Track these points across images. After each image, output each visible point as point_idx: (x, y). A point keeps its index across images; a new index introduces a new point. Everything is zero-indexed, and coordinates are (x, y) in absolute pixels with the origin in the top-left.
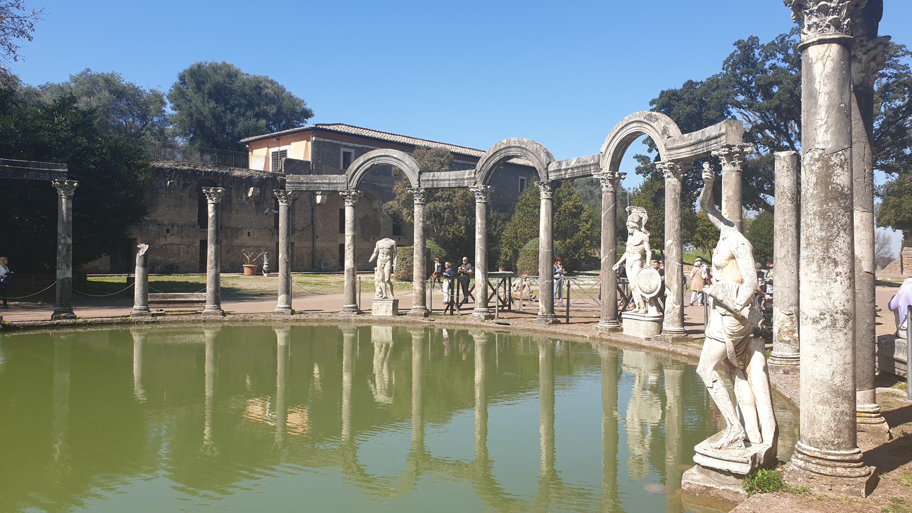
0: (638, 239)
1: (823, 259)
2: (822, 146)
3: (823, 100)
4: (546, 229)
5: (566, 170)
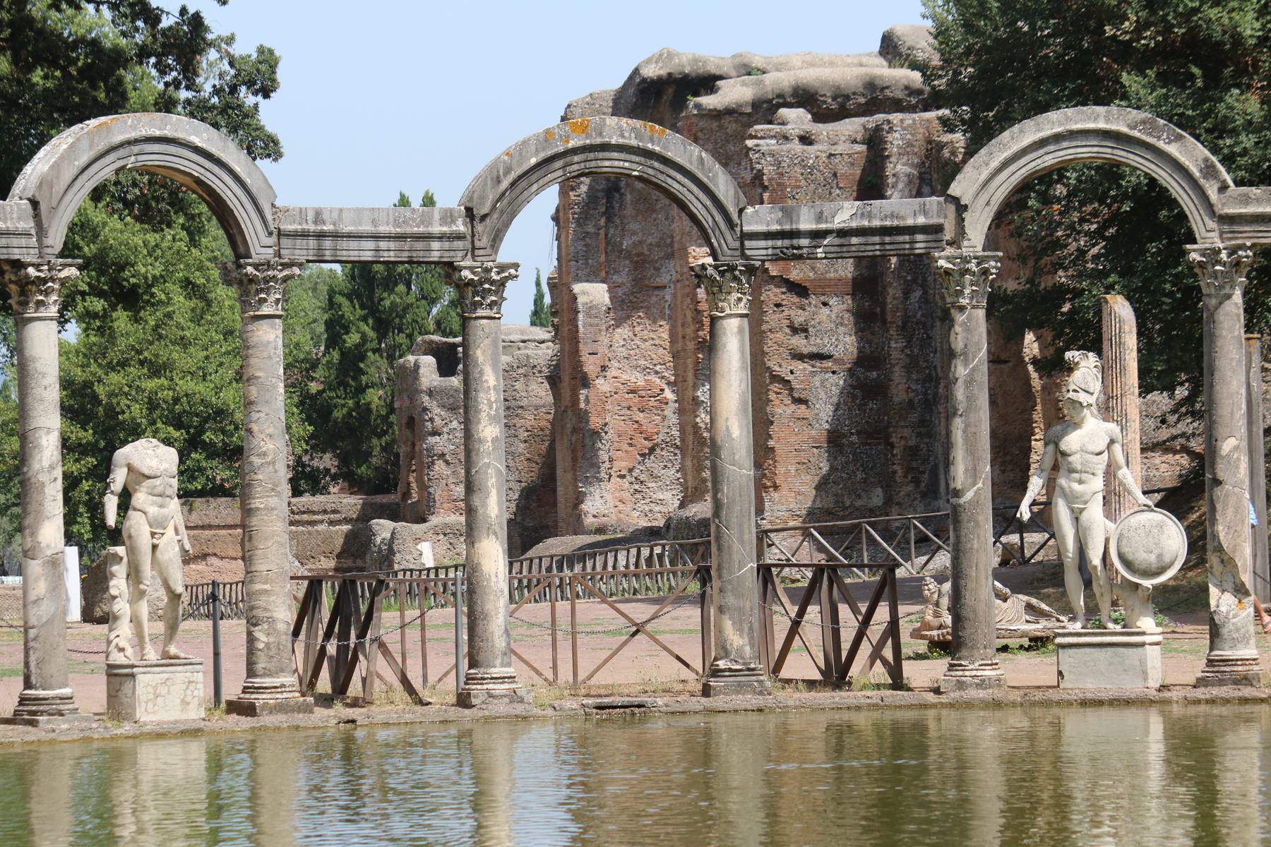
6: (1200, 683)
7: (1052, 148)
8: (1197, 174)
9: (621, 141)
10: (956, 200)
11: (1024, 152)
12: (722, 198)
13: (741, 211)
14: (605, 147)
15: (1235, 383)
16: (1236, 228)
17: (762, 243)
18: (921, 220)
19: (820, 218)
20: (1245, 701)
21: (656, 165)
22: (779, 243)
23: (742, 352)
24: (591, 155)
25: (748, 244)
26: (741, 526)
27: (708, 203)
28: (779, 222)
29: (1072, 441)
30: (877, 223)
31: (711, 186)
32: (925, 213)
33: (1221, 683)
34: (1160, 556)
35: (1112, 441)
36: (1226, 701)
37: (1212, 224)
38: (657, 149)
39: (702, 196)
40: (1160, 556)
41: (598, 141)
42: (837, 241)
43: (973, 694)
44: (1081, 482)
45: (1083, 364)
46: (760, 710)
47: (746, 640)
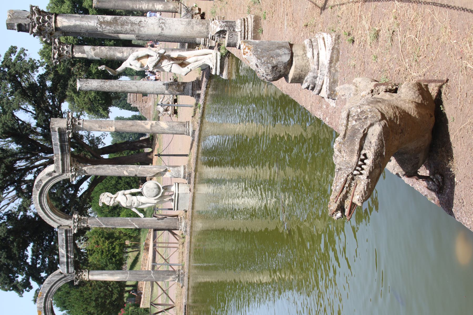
0: (122, 198)
1: (139, 25)
2: (96, 24)
3: (78, 23)
4: (112, 274)
5: (68, 257)
6: (189, 183)
7: (44, 207)
8: (51, 178)
9: (43, 303)
10: (58, 227)
11: (45, 213)
12: (58, 279)
13: (61, 273)
14: (45, 307)
15: (109, 171)
16: (66, 169)
17: (70, 269)
18: (64, 234)
19: (63, 256)
20: (195, 177)
21: (49, 294)
22: (70, 265)
23: (98, 275)
24: (47, 310)
25: (70, 272)
26: (142, 277)
27: (59, 282)
28: (64, 265)
29: (124, 204)
30: (65, 244)
31: (55, 281)
32: (62, 233)
33: (190, 179)
34: (155, 188)
35: (124, 195)
36: (195, 181)
37: (65, 175)
38: (45, 295)
39: (57, 284)
40: (155, 188)
41: (43, 309)
42: (69, 253)
43: (188, 229)
44: (134, 204)
45: (103, 201)
46: (189, 278)
47: (171, 277)
